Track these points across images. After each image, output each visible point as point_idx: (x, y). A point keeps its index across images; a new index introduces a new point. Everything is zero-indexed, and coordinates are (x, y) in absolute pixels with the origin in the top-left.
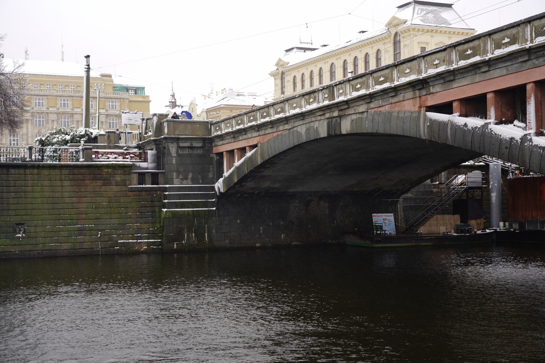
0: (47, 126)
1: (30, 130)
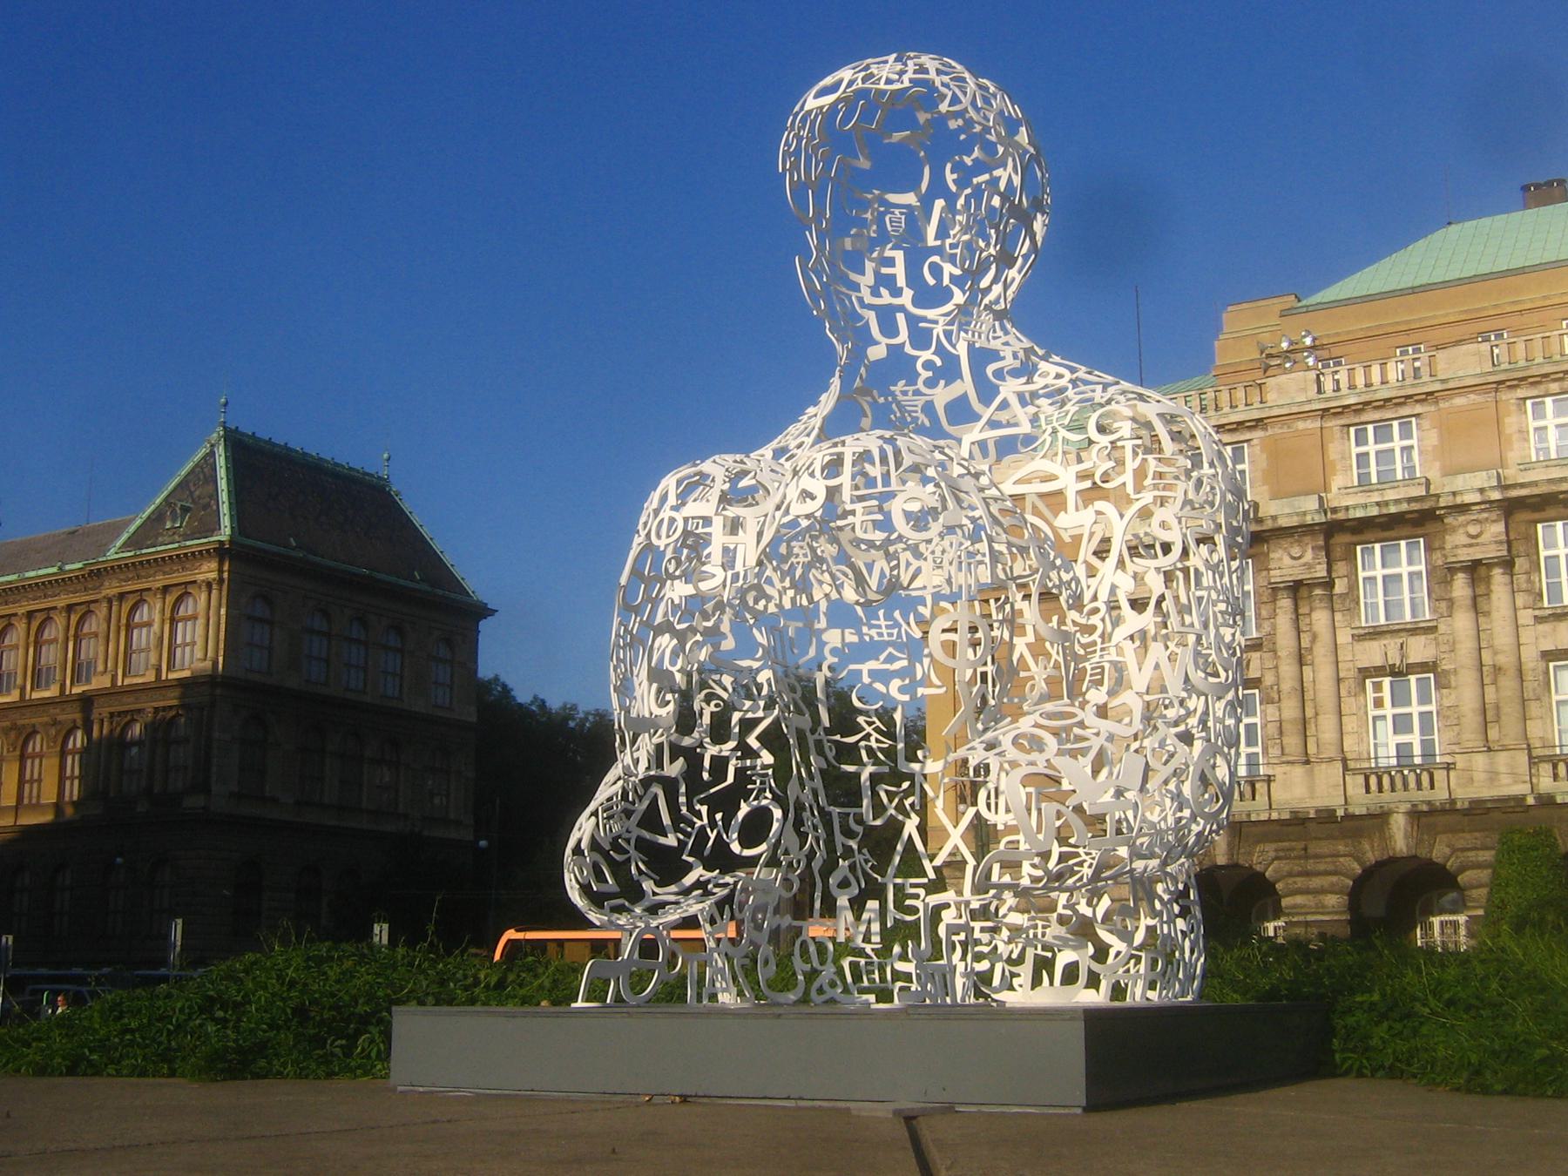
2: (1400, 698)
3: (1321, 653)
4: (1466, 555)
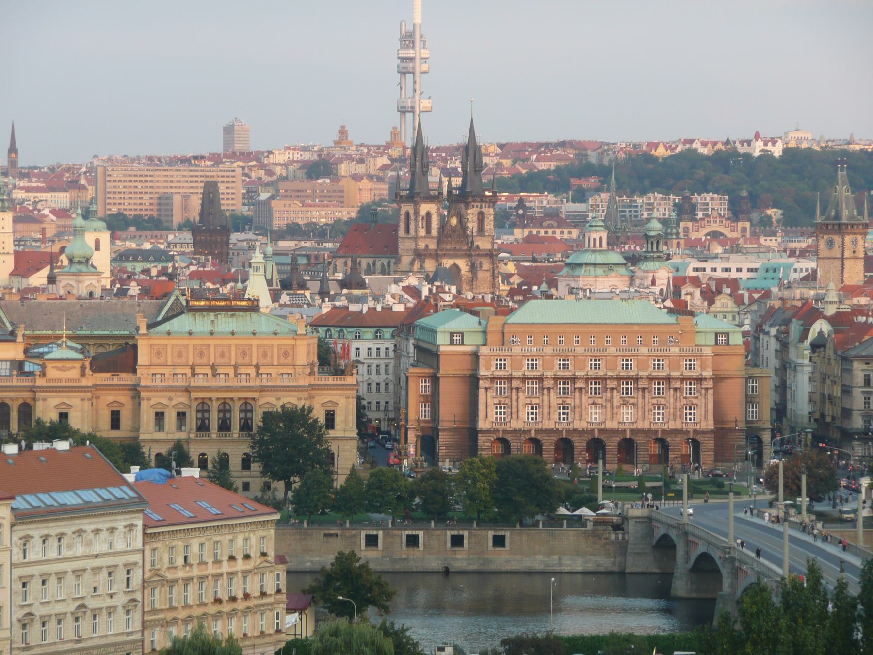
2: (532, 408)
3: (520, 400)
4: (547, 386)
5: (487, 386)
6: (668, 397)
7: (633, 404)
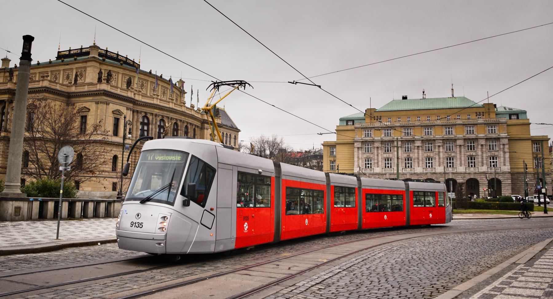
0: (434, 150)
1: (420, 155)
3: (379, 155)
5: (360, 146)
6: (477, 152)
7: (454, 156)
